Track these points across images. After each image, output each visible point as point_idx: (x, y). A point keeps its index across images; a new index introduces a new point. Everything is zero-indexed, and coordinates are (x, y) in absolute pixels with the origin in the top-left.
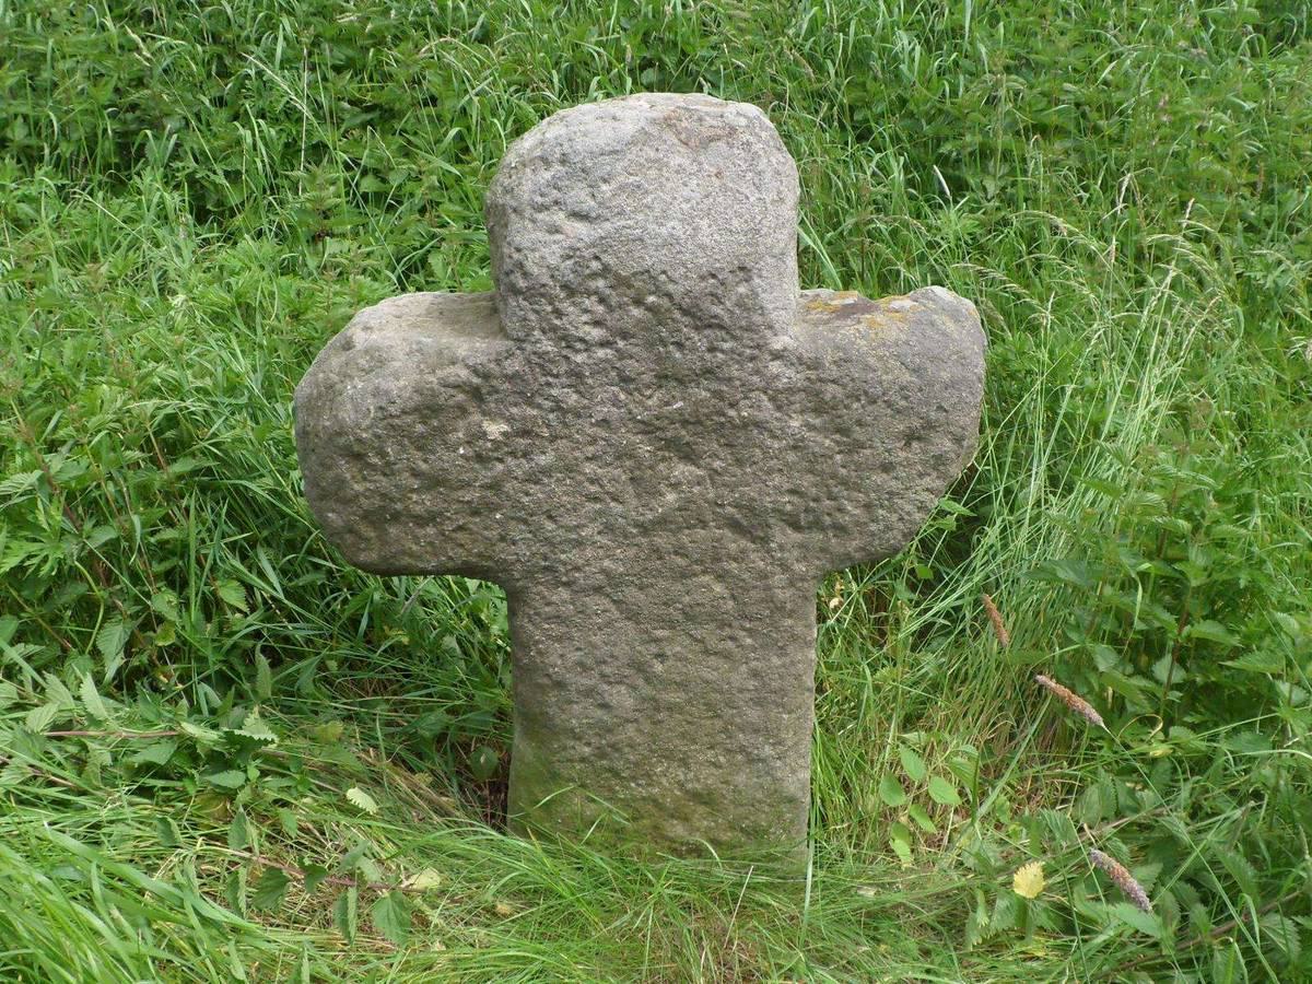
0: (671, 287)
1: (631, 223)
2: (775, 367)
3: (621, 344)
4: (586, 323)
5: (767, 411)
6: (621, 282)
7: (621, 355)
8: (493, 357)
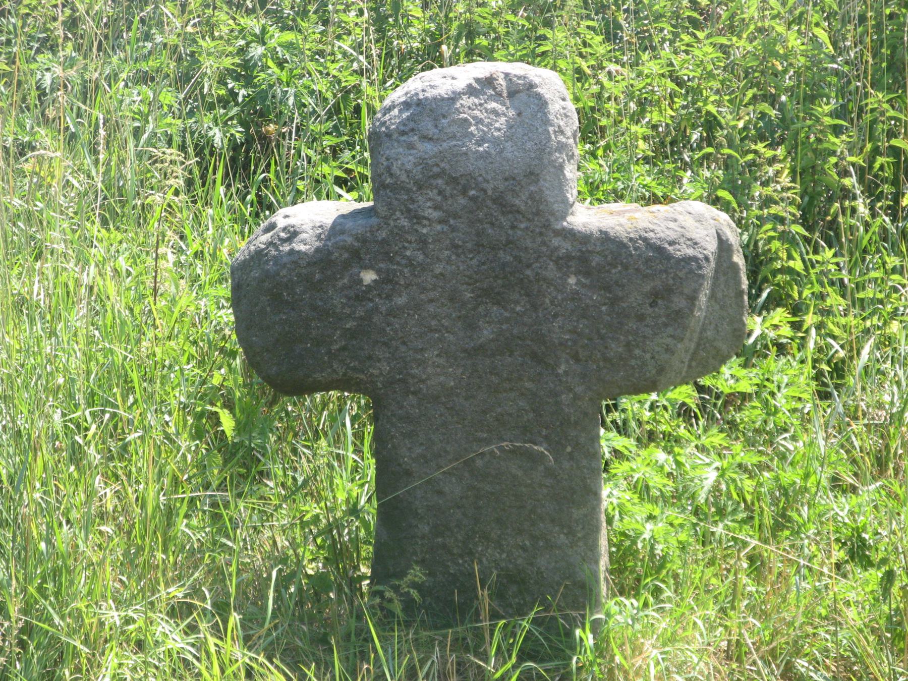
0: (485, 185)
1: (460, 143)
2: (556, 242)
3: (452, 222)
4: (429, 207)
5: (551, 272)
6: (454, 181)
7: (453, 229)
8: (368, 229)
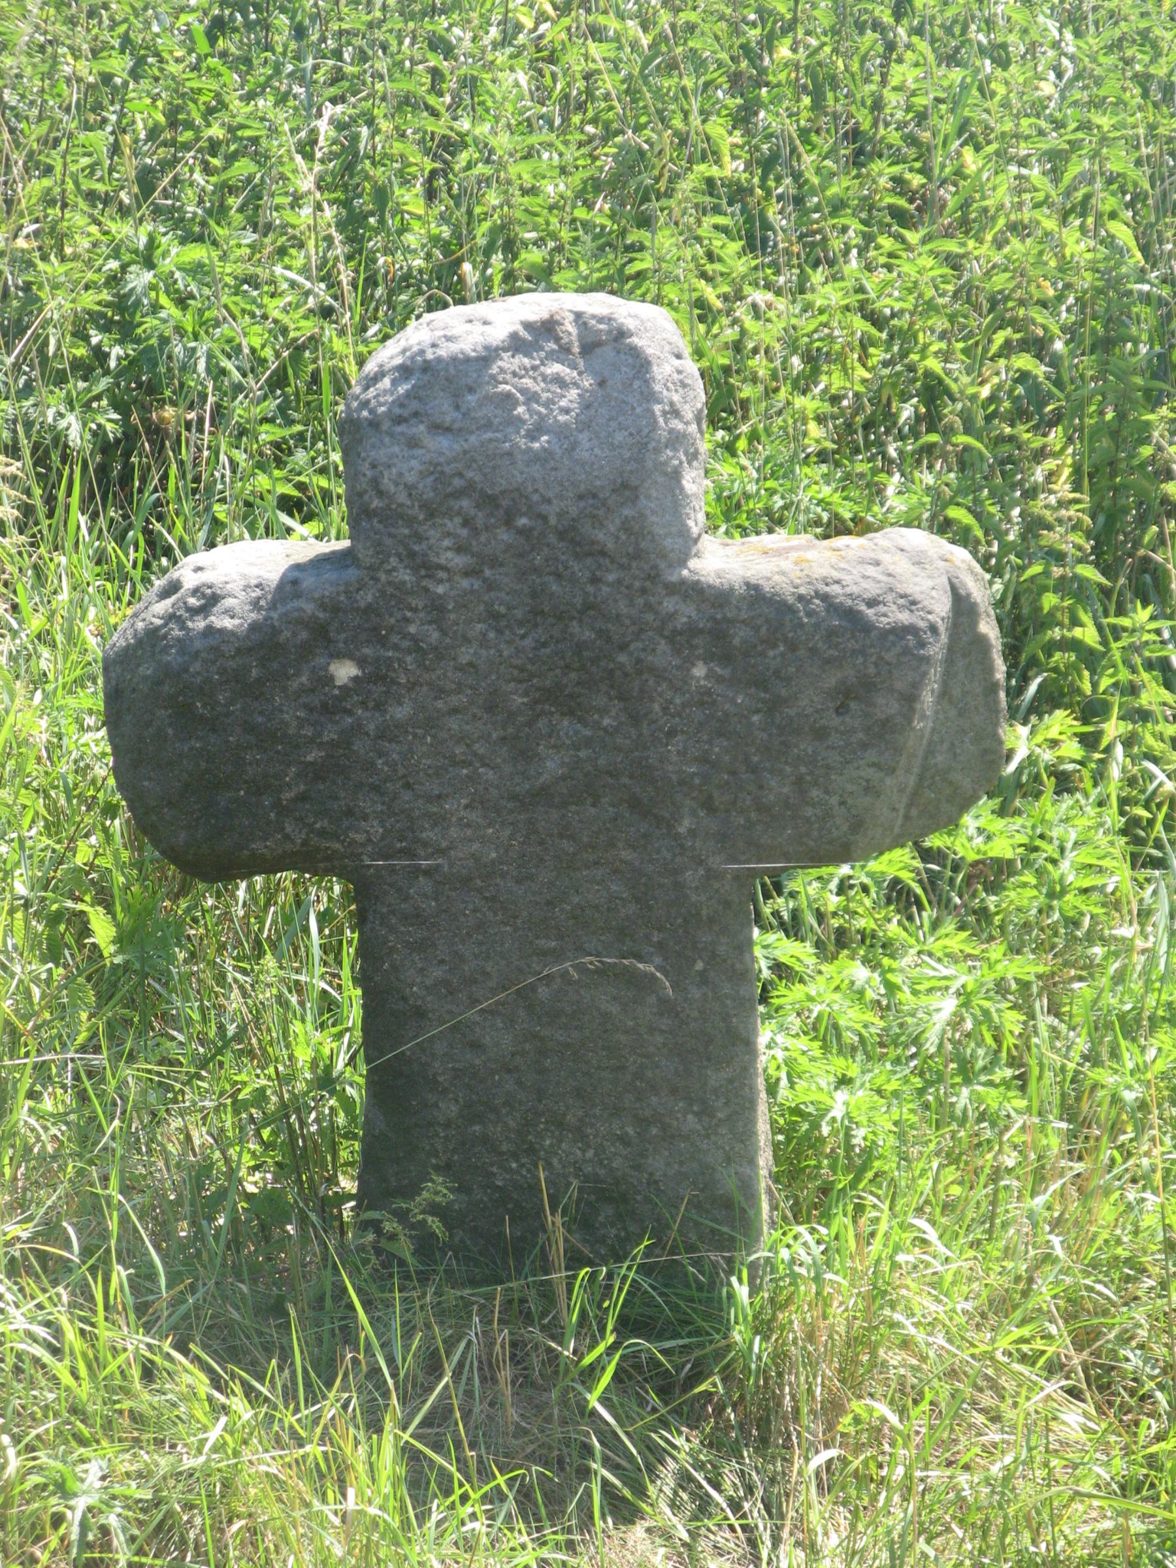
0: (544, 509)
3: (488, 573)
5: (663, 655)
6: (489, 501)
7: (490, 586)
